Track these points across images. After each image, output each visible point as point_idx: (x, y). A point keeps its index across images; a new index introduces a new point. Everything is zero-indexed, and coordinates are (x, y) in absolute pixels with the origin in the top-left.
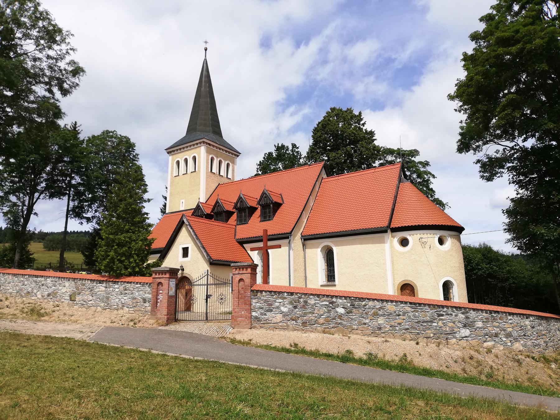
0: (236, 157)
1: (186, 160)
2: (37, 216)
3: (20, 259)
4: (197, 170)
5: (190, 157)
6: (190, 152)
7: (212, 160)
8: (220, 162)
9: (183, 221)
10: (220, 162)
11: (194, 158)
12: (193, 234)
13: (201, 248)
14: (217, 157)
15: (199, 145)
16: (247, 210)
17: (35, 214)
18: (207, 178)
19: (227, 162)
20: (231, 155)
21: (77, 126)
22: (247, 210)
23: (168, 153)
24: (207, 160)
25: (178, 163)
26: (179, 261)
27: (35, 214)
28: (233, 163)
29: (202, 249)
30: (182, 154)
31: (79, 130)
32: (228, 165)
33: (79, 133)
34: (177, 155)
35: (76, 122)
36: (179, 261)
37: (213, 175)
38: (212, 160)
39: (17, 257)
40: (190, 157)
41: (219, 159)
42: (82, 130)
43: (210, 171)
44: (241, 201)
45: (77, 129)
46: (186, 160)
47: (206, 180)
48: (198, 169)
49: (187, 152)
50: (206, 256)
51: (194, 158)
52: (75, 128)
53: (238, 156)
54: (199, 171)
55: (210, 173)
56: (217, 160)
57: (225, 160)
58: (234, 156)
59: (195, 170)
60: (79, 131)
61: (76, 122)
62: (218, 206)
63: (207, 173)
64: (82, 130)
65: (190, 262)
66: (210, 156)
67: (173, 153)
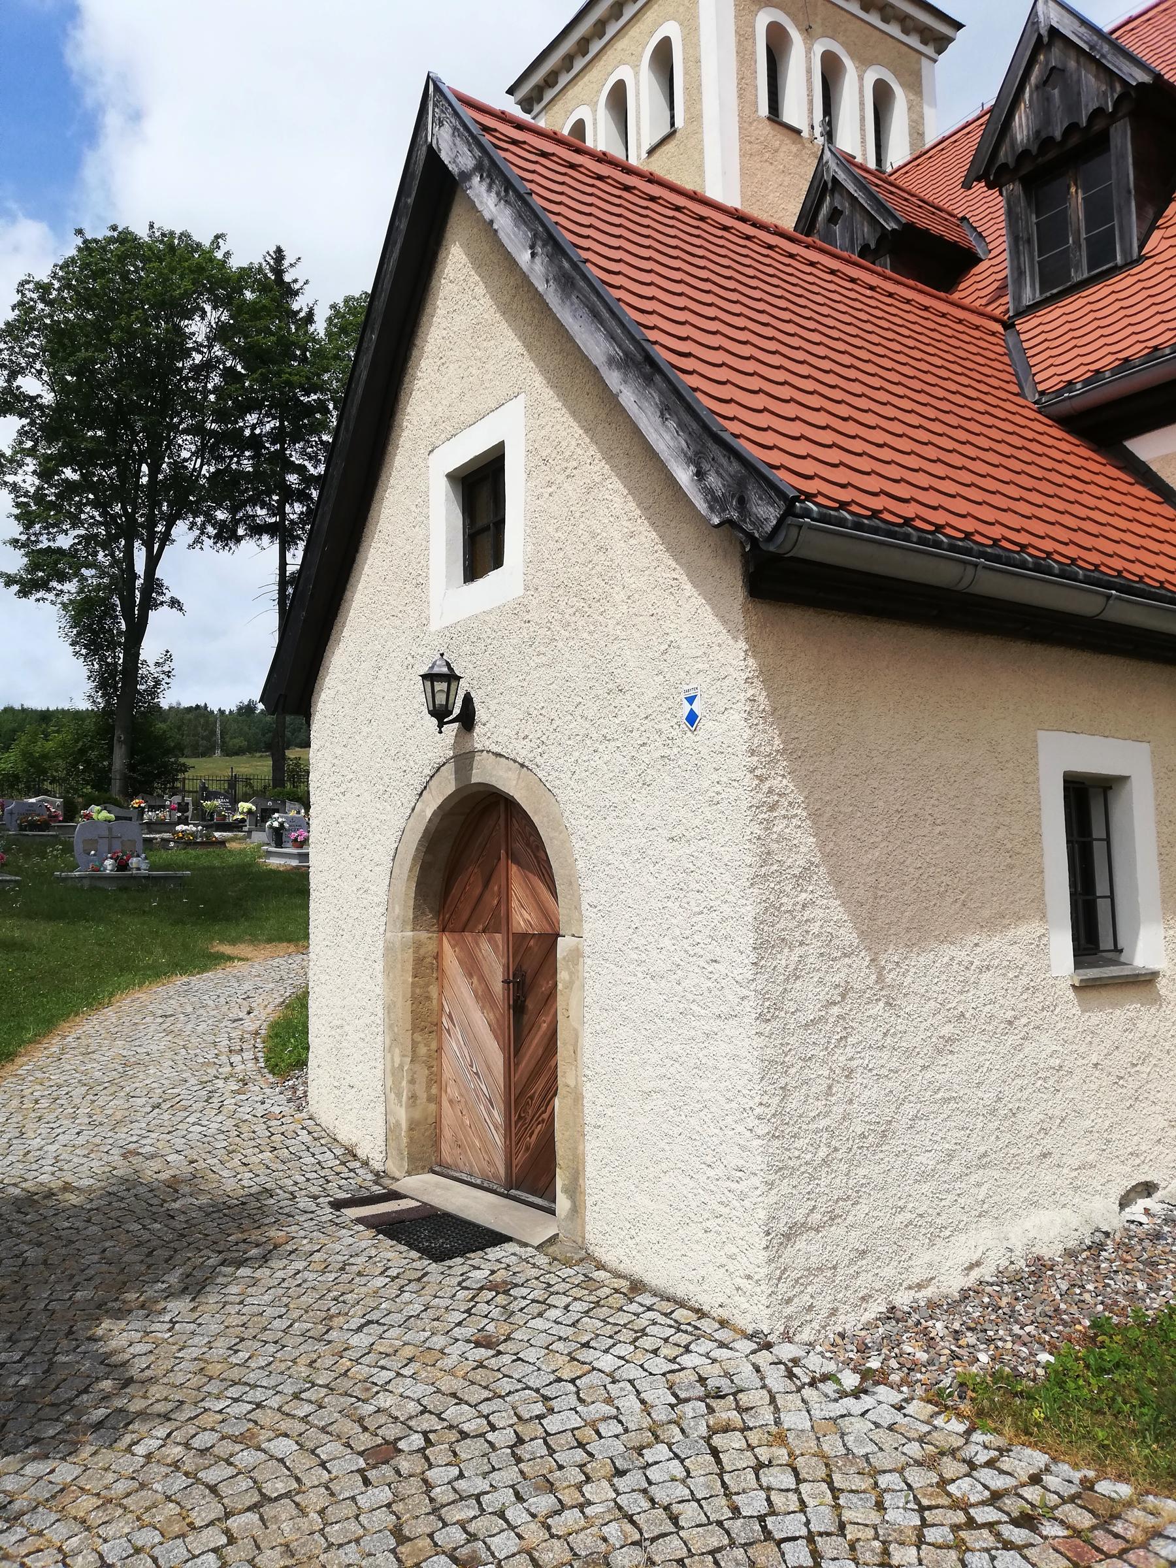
0: (929, 50)
2: (181, 609)
3: (132, 767)
4: (679, 123)
5: (636, 67)
6: (634, 32)
9: (433, 155)
12: (533, 265)
13: (613, 378)
14: (808, 31)
16: (1122, 139)
17: (175, 603)
18: (743, 154)
19: (871, 77)
20: (894, 30)
21: (286, 263)
22: (1122, 139)
24: (744, 37)
26: (435, 625)
27: (175, 603)
28: (915, 84)
29: (628, 397)
30: (594, 74)
31: (295, 281)
32: (882, 96)
33: (296, 293)
34: (571, 93)
35: (279, 250)
36: (435, 625)
37: (788, 146)
39: (119, 760)
40: (636, 67)
41: (819, 49)
42: (306, 282)
43: (764, 110)
44: (1053, 75)
45: (287, 278)
47: (744, 172)
48: (687, 110)
49: (621, 44)
50: (684, 475)
52: (279, 272)
53: (941, 43)
54: (695, 118)
55: (767, 129)
56: (809, 51)
57: (864, 63)
58: (914, 41)
59: (672, 124)
60: (296, 286)
61: (279, 250)
62: (835, 215)
63: (745, 120)
64: (306, 282)
65: (518, 609)
66: (763, 19)
67: (549, 95)
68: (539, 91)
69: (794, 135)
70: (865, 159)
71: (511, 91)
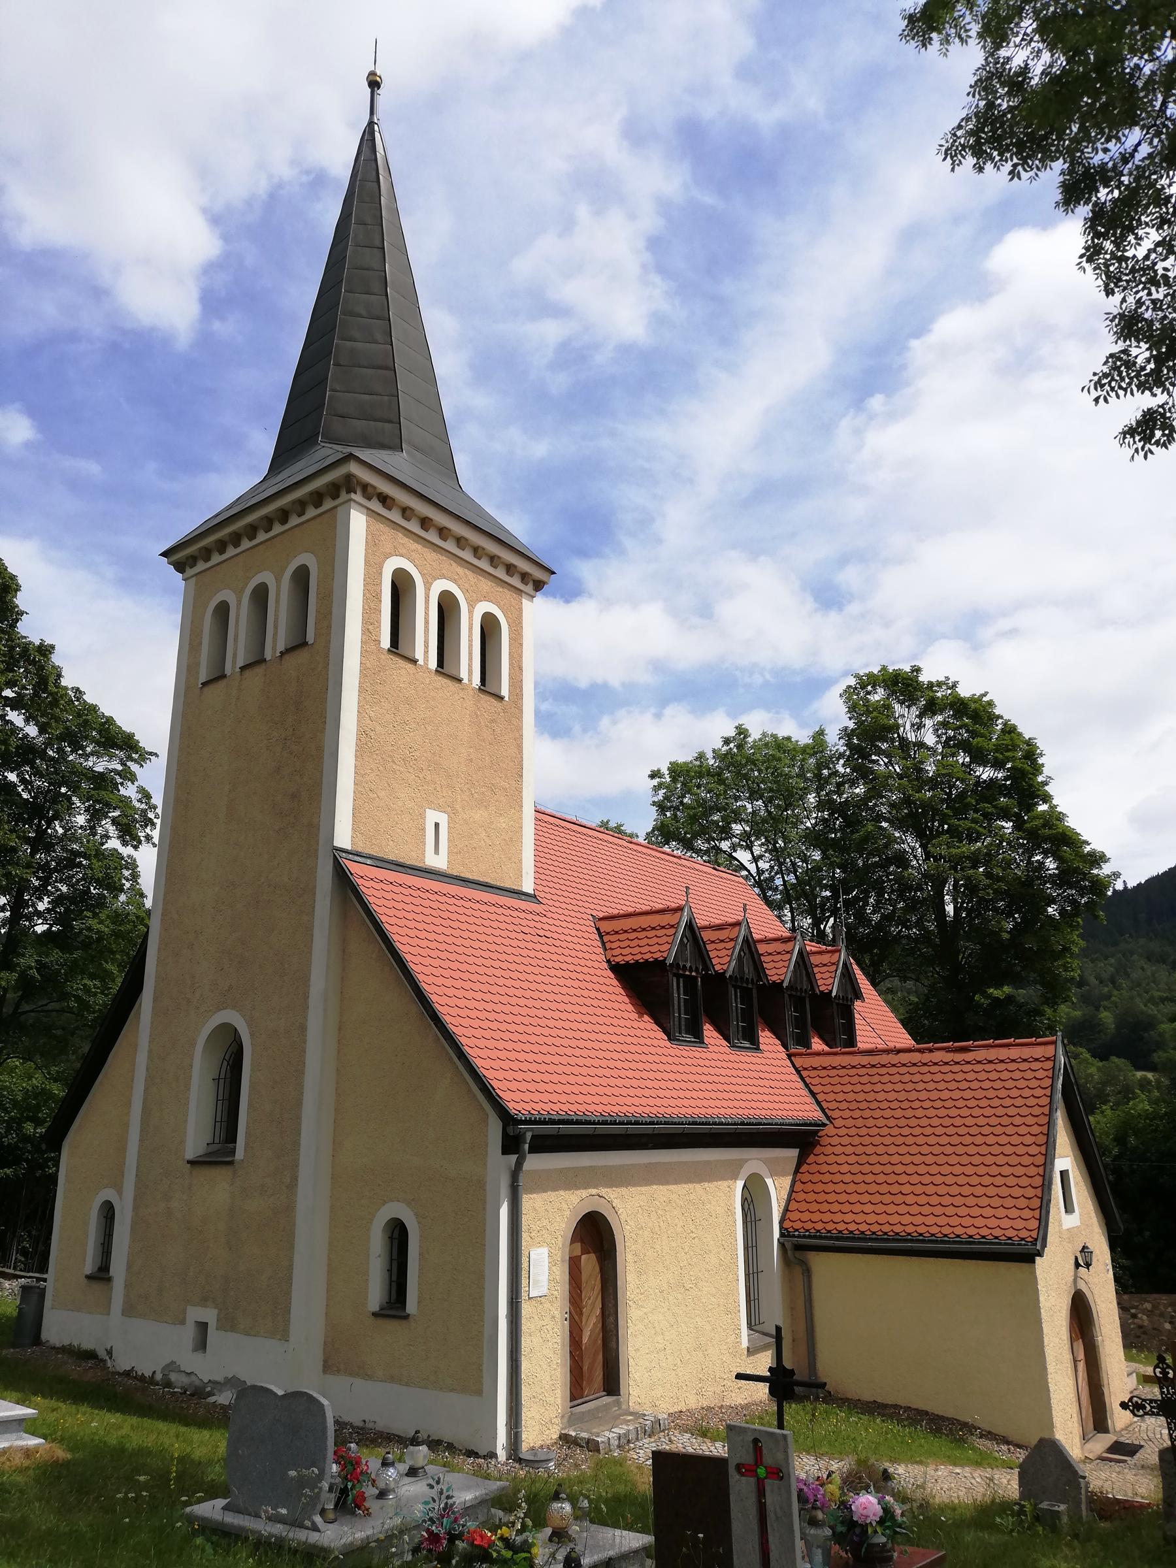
0: (529, 588)
1: (261, 596)
4: (310, 638)
5: (278, 581)
7: (401, 589)
8: (447, 610)
10: (447, 610)
11: (302, 577)
15: (328, 504)
23: (180, 567)
25: (223, 610)
38: (401, 589)
40: (278, 581)
43: (386, 643)
46: (261, 596)
51: (302, 577)
68: (192, 560)
69: (409, 666)
70: (470, 680)
71: (164, 554)
